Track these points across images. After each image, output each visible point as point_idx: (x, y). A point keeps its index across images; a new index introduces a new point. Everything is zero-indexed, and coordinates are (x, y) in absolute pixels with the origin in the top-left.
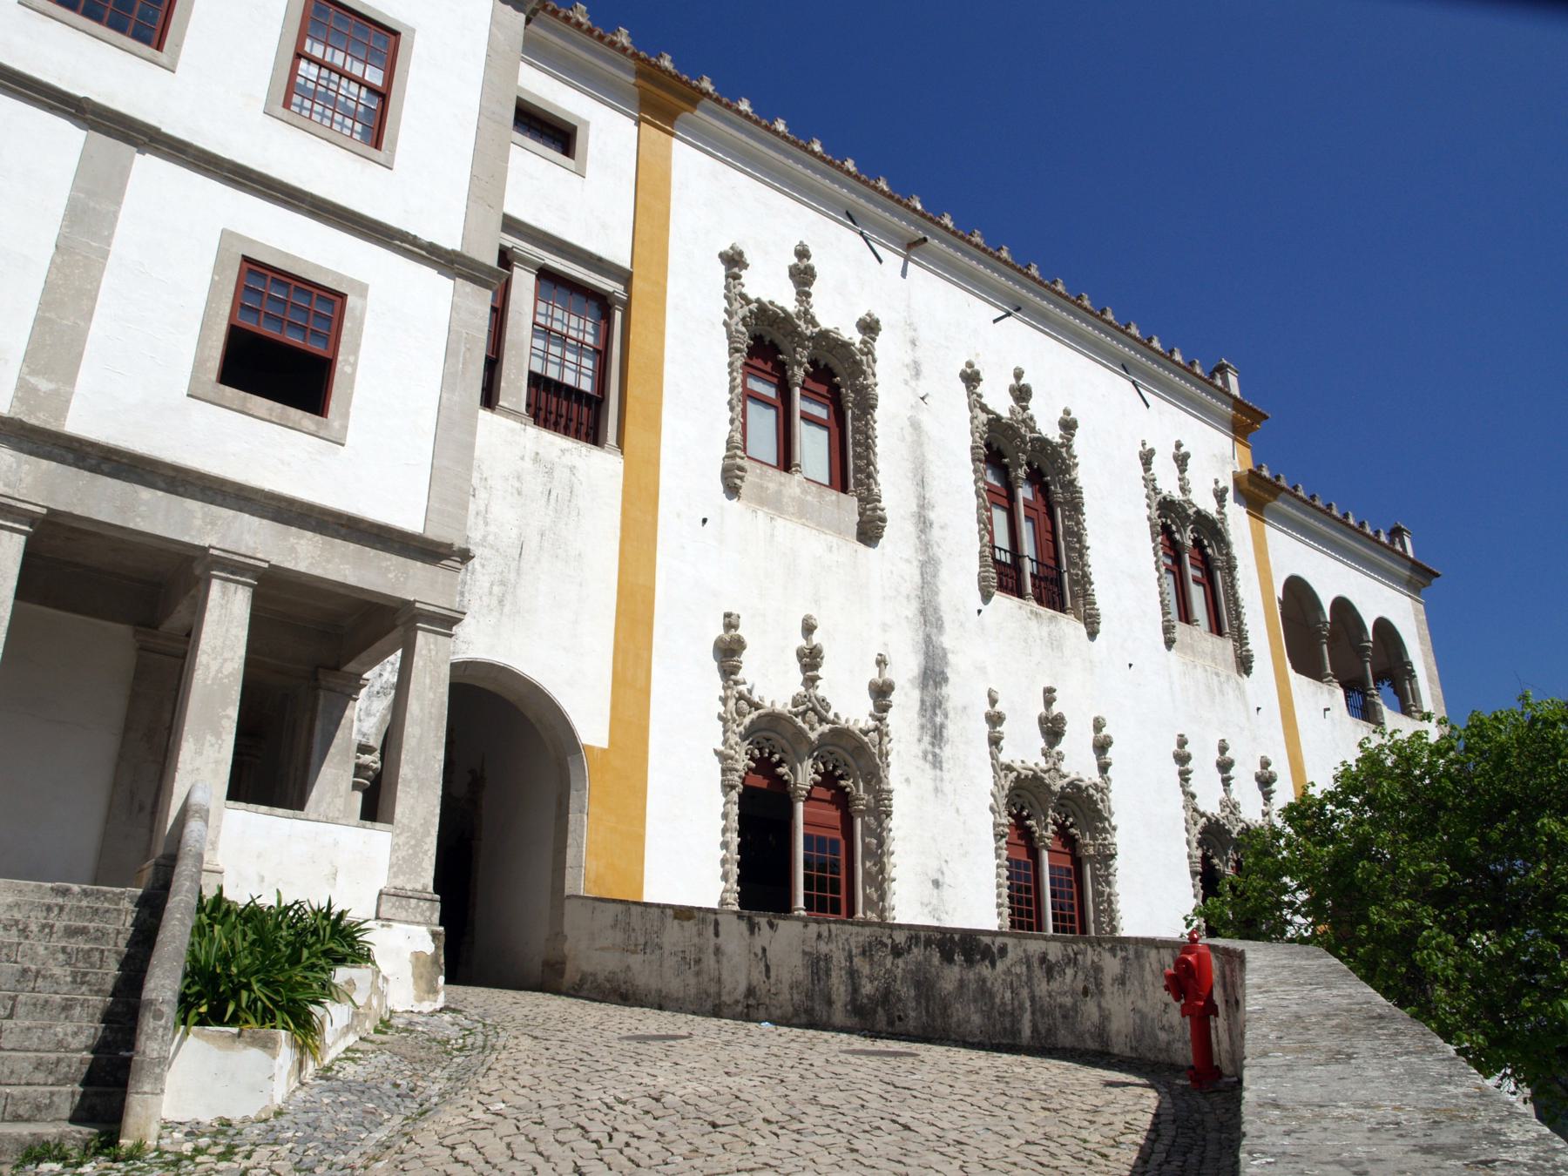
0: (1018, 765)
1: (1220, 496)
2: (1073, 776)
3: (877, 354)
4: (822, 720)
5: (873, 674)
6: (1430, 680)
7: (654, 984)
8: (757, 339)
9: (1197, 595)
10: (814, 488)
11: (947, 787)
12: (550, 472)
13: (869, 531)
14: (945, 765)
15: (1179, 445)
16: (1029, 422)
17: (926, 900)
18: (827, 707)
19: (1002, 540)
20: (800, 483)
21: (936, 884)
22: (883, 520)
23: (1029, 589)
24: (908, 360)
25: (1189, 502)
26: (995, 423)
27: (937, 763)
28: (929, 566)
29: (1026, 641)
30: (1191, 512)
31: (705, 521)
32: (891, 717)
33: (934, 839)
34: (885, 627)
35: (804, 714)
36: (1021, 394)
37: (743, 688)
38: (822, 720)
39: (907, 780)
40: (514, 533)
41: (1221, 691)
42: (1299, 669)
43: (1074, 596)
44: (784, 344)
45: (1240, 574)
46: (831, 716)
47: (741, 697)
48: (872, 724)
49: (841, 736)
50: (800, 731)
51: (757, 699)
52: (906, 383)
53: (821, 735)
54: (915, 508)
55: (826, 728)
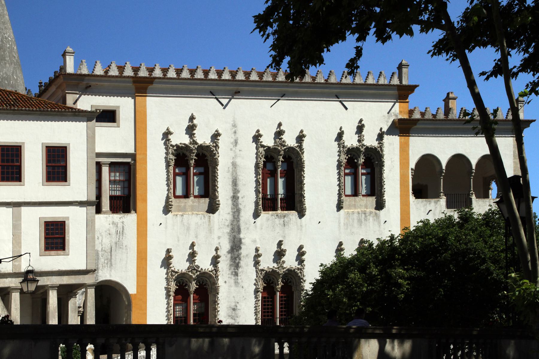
0: (266, 269)
2: (288, 267)
3: (219, 145)
4: (197, 271)
5: (214, 253)
10: (197, 200)
11: (239, 281)
12: (117, 226)
14: (239, 275)
16: (283, 144)
17: (230, 314)
18: (198, 267)
20: (192, 200)
21: (234, 309)
22: (219, 204)
24: (232, 140)
26: (268, 150)
27: (236, 274)
28: (236, 211)
29: (273, 227)
30: (362, 149)
31: (161, 224)
32: (219, 265)
33: (234, 297)
34: (219, 238)
35: (191, 271)
37: (173, 269)
38: (197, 271)
39: (225, 282)
40: (109, 246)
41: (365, 220)
44: (187, 154)
46: (200, 269)
47: (172, 271)
48: (213, 268)
49: (205, 273)
50: (191, 276)
51: (176, 270)
52: (231, 149)
53: (197, 276)
54: (232, 194)
55: (198, 273)
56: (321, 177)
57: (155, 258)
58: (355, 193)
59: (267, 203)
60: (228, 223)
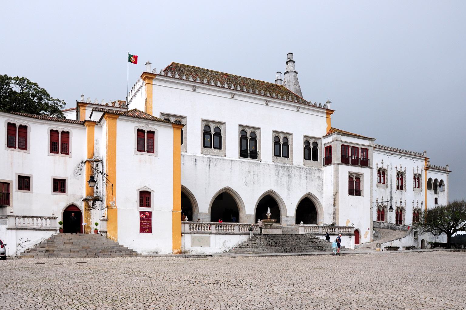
1: (422, 171)
6: (447, 186)
7: (376, 226)
8: (378, 170)
9: (417, 183)
13: (387, 187)
15: (417, 166)
19: (398, 184)
23: (400, 188)
25: (418, 173)
26: (399, 172)
28: (391, 189)
36: (401, 167)
42: (428, 189)
43: (404, 188)
45: (422, 180)
56: (409, 181)
57: (375, 200)
58: (415, 187)
59: (398, 187)
60: (390, 192)
